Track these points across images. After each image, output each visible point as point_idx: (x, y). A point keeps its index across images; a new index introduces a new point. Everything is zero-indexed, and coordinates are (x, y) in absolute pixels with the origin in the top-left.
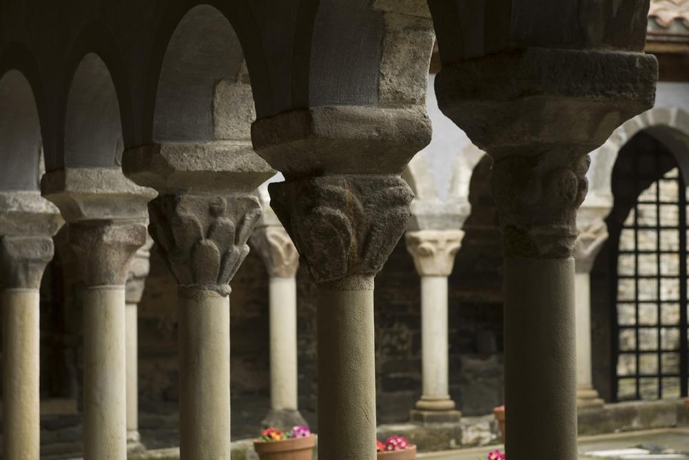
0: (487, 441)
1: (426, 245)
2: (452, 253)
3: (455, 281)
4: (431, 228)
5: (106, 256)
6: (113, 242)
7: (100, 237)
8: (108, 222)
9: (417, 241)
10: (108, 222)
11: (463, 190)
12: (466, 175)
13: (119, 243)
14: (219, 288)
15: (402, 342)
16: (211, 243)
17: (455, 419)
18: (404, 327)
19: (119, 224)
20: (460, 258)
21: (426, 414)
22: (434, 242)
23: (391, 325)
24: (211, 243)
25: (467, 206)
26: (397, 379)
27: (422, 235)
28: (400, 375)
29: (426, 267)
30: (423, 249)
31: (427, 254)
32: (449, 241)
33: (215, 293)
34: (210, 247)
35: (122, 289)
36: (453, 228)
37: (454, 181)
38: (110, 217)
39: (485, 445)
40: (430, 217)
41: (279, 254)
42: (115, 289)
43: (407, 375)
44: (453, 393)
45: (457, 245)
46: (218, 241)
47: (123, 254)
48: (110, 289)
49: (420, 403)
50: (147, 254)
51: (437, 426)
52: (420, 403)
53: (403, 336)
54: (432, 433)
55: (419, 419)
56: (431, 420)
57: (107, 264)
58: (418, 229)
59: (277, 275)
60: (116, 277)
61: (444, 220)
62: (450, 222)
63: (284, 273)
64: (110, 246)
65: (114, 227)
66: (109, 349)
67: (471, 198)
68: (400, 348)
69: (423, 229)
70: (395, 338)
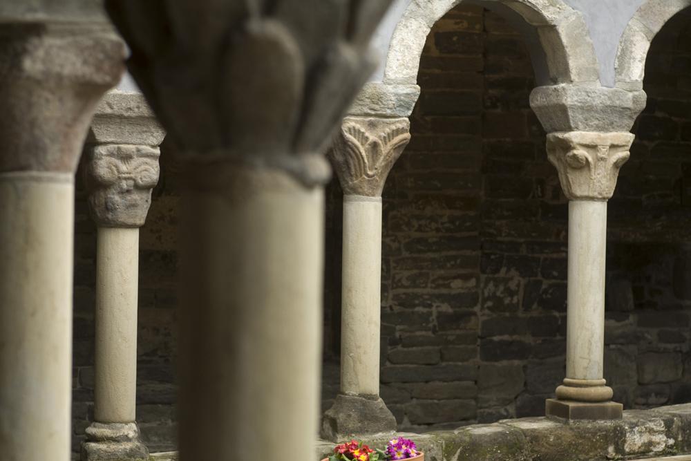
0: (661, 448)
1: (581, 152)
2: (616, 165)
3: (617, 210)
4: (588, 127)
5: (30, 106)
6: (47, 74)
7: (16, 62)
8: (37, 29)
9: (566, 146)
10: (37, 29)
11: (637, 71)
12: (641, 48)
13: (60, 78)
14: (294, 163)
15: (511, 293)
16: (276, 30)
17: (616, 415)
18: (513, 272)
19: (61, 34)
20: (626, 172)
21: (571, 405)
22: (592, 147)
23: (497, 271)
24: (276, 30)
25: (643, 95)
26: (501, 343)
27: (575, 136)
28: (506, 337)
29: (579, 185)
30: (575, 156)
31: (582, 166)
32: (613, 147)
33: (286, 181)
34: (273, 46)
35: (67, 181)
36: (621, 128)
37: (624, 56)
38: (40, 16)
39: (658, 455)
40: (587, 109)
41: (359, 157)
42: (51, 180)
43: (515, 337)
44: (611, 370)
45: (624, 153)
46: (299, 28)
47: (70, 104)
48: (38, 180)
49: (561, 389)
50: (158, 151)
51: (588, 425)
52: (561, 389)
53: (512, 285)
54: (581, 434)
55: (560, 412)
56: (580, 414)
57: (33, 124)
58: (570, 129)
59: (355, 191)
60: (53, 153)
61: (607, 116)
62: (615, 118)
63: (366, 188)
64: (39, 83)
65: (49, 41)
66: (33, 314)
67: (648, 83)
68: (507, 301)
69: (577, 128)
70: (501, 288)
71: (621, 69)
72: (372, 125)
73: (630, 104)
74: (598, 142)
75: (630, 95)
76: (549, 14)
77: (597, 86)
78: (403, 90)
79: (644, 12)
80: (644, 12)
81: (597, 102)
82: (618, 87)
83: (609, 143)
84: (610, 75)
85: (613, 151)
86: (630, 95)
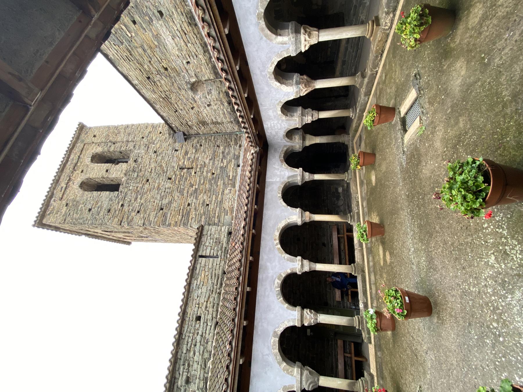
32: (305, 41)
36: (300, 38)
61: (297, 42)
71: (286, 44)
72: (302, 90)
73: (294, 39)
74: (304, 45)
75: (292, 39)
76: (276, 64)
77: (291, 48)
78: (295, 88)
79: (271, 40)
80: (271, 40)
81: (294, 48)
82: (290, 43)
83: (304, 42)
84: (287, 45)
85: (306, 39)
86: (292, 39)
